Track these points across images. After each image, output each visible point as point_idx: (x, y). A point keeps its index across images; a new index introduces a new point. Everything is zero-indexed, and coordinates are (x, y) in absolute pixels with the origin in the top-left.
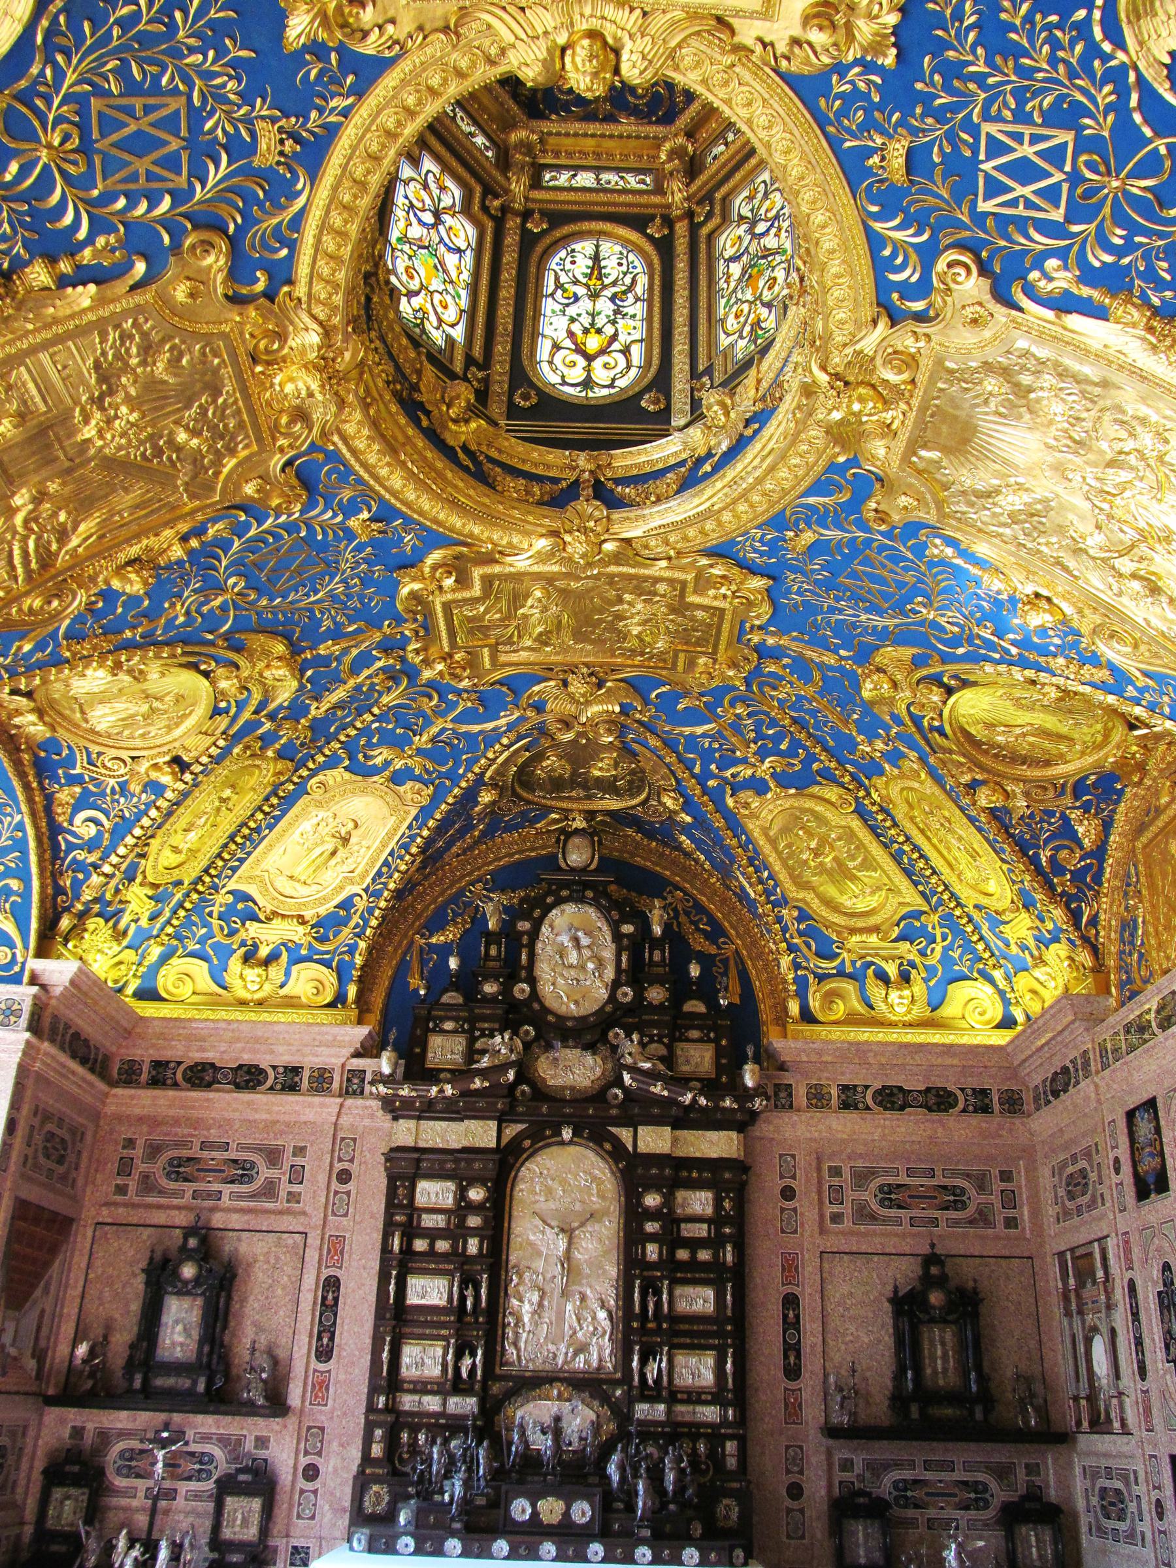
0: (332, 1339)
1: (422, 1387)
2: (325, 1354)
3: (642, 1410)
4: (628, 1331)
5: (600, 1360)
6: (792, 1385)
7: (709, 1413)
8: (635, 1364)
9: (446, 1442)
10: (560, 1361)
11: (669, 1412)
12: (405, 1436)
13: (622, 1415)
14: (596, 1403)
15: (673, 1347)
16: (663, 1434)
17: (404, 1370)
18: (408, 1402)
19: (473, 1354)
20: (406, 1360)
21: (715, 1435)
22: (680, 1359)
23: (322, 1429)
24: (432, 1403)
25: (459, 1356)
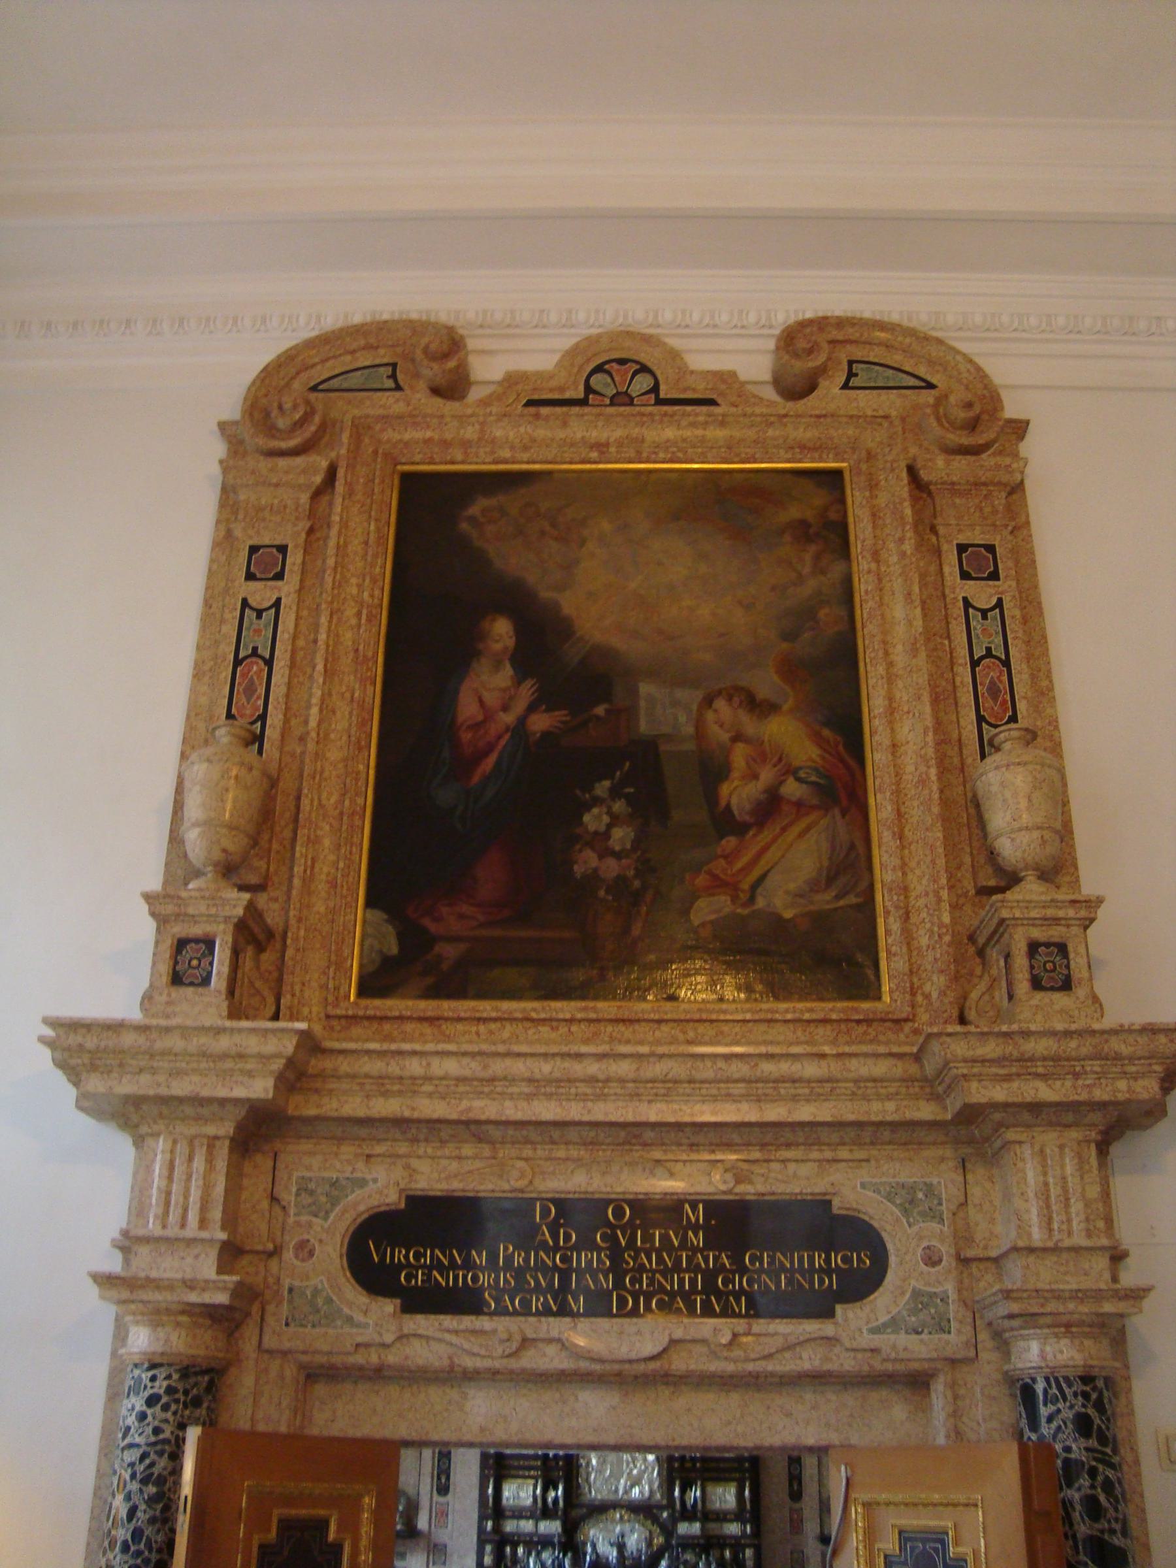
0: (448, 1478)
1: (519, 1514)
2: (443, 1490)
3: (683, 1528)
4: (670, 1470)
5: (651, 1491)
6: (797, 1506)
7: (733, 1528)
8: (677, 1493)
9: (538, 1554)
10: (621, 1492)
11: (703, 1529)
12: (508, 1549)
13: (668, 1531)
14: (649, 1522)
15: (704, 1481)
16: (698, 1545)
17: (504, 1502)
18: (510, 1526)
19: (556, 1489)
20: (506, 1493)
21: (737, 1545)
22: (709, 1489)
23: (445, 1546)
24: (527, 1526)
25: (545, 1491)
